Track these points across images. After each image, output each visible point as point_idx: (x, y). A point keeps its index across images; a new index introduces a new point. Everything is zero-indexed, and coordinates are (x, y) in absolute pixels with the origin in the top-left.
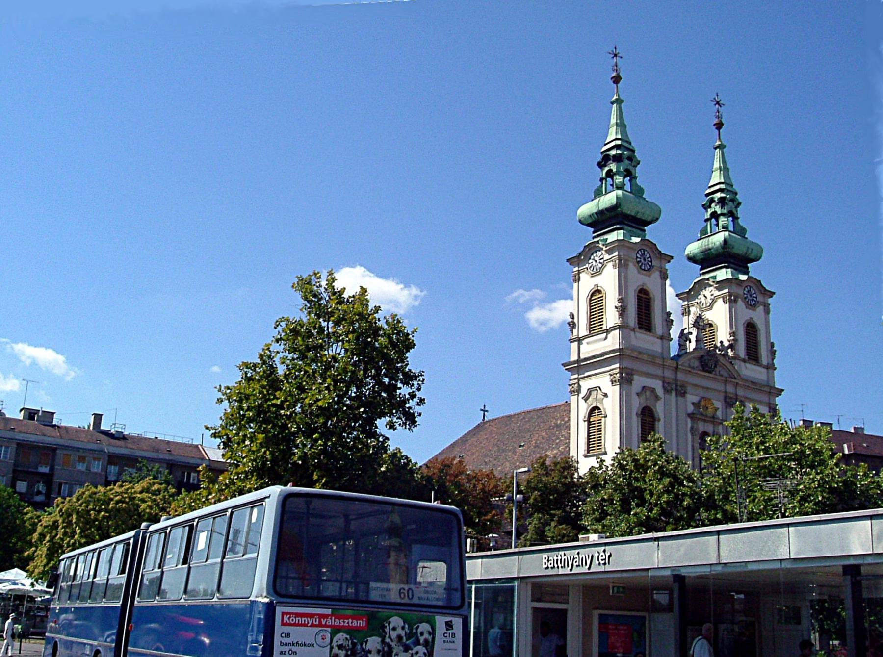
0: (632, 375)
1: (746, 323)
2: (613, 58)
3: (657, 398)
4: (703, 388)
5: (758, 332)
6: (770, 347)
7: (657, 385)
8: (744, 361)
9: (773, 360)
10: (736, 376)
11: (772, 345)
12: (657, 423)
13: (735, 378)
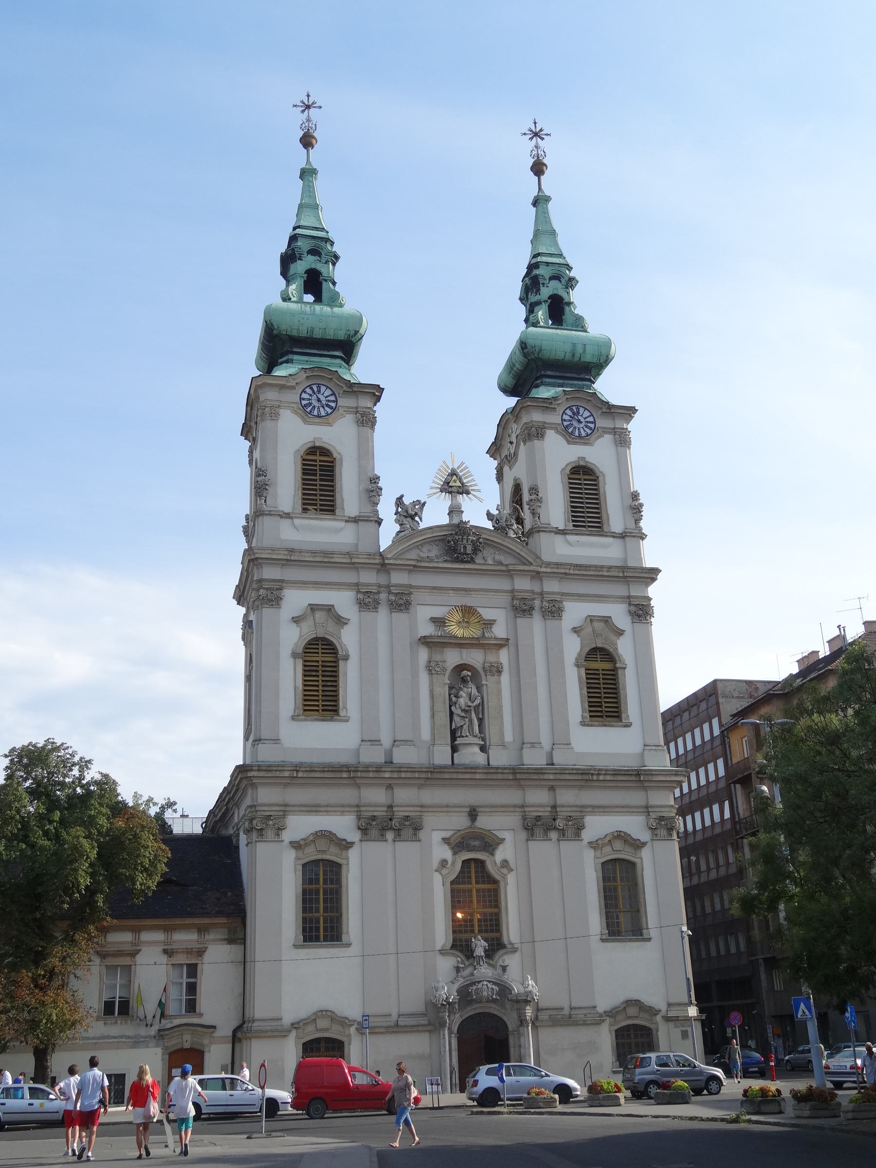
0: (281, 589)
1: (569, 468)
2: (303, 111)
3: (341, 621)
5: (601, 479)
6: (629, 501)
8: (563, 532)
9: (638, 520)
10: (530, 560)
11: (635, 496)
12: (341, 663)
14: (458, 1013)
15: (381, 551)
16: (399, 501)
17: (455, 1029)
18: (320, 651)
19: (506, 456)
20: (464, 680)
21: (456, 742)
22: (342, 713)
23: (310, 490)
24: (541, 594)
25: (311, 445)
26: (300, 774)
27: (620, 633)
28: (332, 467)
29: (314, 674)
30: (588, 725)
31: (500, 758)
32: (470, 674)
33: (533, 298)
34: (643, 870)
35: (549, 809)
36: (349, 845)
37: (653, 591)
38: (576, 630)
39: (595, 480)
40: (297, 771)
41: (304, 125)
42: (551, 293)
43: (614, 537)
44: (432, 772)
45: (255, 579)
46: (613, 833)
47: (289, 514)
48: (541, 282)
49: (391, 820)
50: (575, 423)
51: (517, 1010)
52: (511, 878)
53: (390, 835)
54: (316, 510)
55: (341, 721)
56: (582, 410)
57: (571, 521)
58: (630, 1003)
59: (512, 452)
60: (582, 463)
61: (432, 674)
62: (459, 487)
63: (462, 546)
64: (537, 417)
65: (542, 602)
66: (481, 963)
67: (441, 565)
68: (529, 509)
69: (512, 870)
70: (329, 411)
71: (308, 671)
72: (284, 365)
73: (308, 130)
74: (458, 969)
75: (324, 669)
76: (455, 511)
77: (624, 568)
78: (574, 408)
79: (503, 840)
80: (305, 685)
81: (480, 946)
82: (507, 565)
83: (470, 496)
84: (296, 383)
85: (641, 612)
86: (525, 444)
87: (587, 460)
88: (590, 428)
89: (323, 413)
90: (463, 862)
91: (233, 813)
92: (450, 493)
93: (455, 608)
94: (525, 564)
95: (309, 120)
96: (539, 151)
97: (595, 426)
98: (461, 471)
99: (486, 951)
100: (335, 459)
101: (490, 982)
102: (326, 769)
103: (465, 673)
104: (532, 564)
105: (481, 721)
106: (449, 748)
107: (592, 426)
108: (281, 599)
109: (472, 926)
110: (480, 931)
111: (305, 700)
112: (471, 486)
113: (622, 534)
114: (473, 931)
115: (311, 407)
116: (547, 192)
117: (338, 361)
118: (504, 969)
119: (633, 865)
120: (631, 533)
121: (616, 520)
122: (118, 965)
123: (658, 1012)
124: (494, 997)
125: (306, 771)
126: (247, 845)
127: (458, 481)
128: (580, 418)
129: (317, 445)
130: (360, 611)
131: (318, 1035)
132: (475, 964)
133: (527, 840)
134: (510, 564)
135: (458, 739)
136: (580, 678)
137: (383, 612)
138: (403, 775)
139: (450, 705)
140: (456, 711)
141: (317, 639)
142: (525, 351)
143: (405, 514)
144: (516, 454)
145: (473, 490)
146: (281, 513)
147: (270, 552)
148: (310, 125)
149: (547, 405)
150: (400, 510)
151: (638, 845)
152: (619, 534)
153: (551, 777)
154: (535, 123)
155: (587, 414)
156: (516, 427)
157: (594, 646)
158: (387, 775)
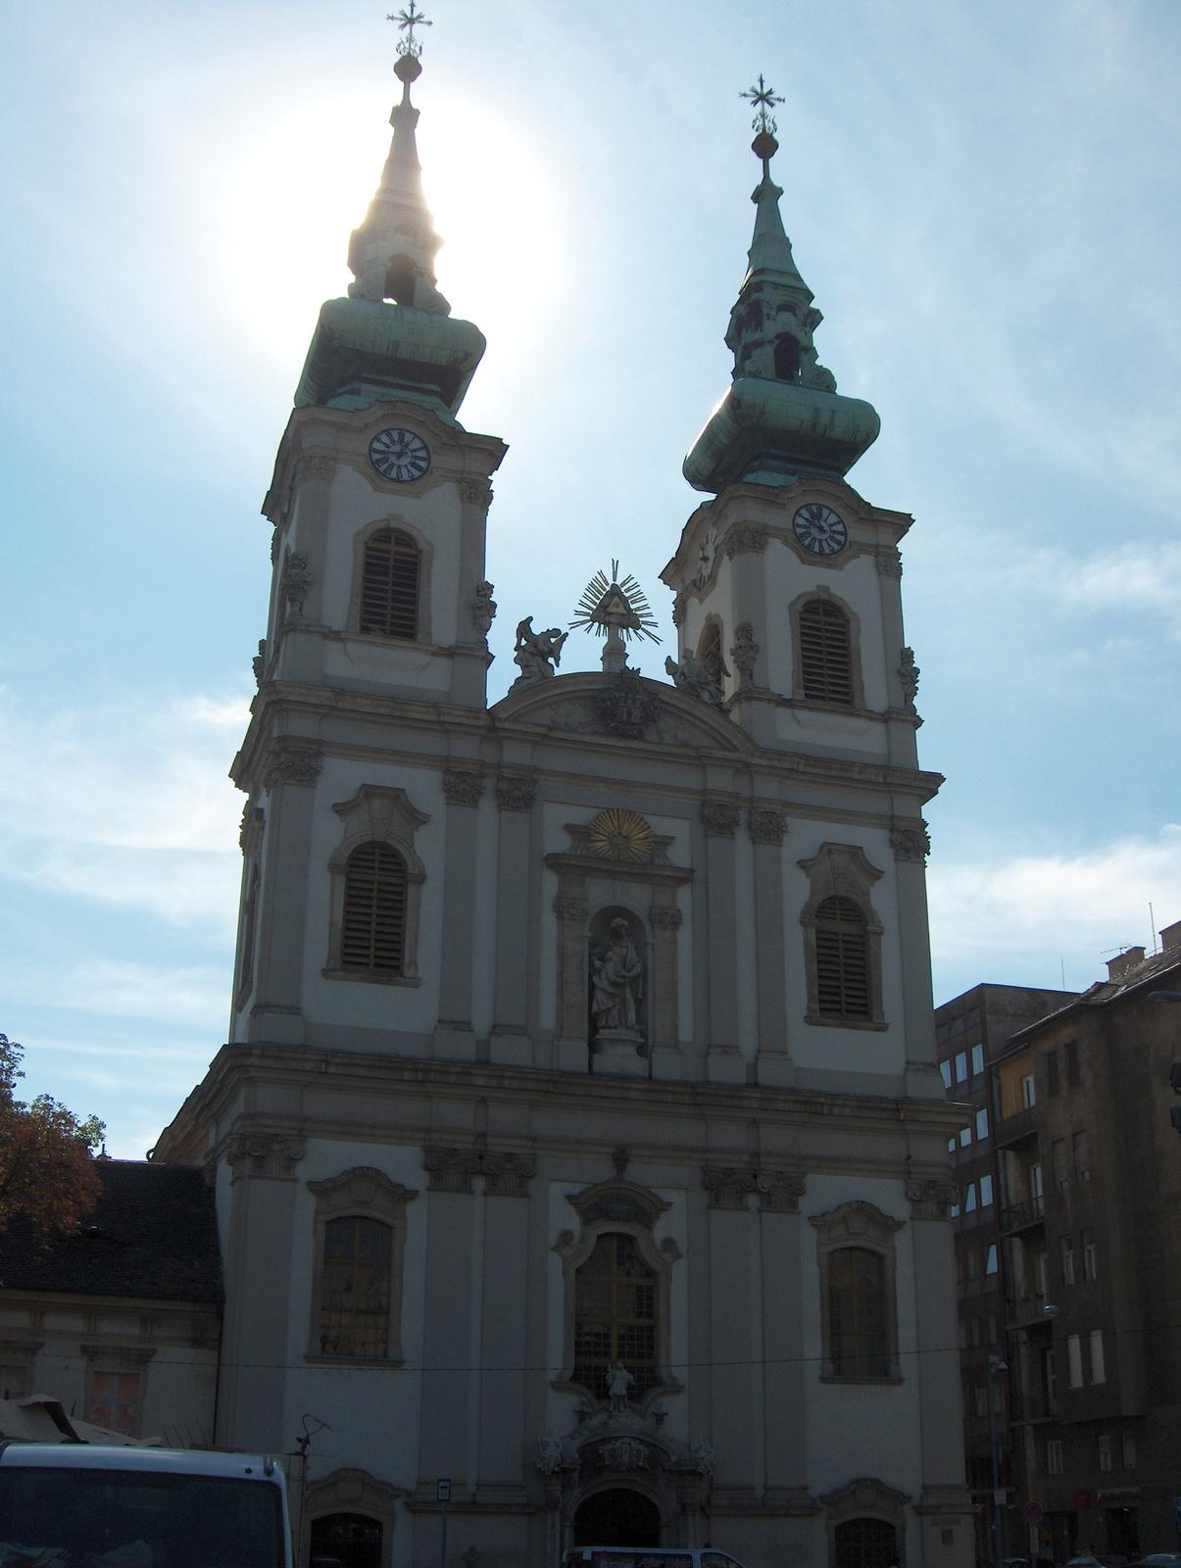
0: (319, 754)
3: (416, 818)
4: (610, 782)
5: (853, 624)
7: (423, 786)
8: (790, 704)
11: (907, 655)
12: (411, 889)
13: (737, 750)
15: (488, 708)
16: (524, 628)
17: (572, 1513)
18: (377, 865)
19: (694, 581)
20: (616, 934)
21: (598, 1037)
22: (408, 972)
23: (376, 590)
24: (751, 800)
25: (382, 525)
26: (332, 1069)
27: (877, 875)
28: (416, 564)
29: (364, 902)
30: (817, 1024)
31: (666, 1066)
32: (626, 923)
33: (749, 337)
34: (895, 1268)
35: (746, 1158)
36: (410, 1195)
37: (928, 811)
38: (803, 865)
39: (843, 626)
40: (328, 1063)
41: (402, 46)
42: (780, 331)
43: (871, 719)
44: (555, 1082)
45: (275, 735)
46: (849, 1204)
47: (339, 633)
48: (765, 311)
49: (481, 1158)
50: (814, 532)
52: (679, 1270)
53: (479, 1183)
54: (384, 631)
55: (405, 985)
56: (825, 513)
57: (802, 686)
58: (862, 1483)
59: (706, 572)
60: (824, 596)
61: (563, 918)
62: (623, 615)
63: (625, 710)
64: (754, 514)
65: (751, 814)
66: (622, 1408)
67: (587, 739)
68: (735, 662)
69: (679, 1256)
70: (417, 473)
71: (355, 898)
72: (346, 396)
73: (409, 53)
74: (582, 1416)
75: (382, 895)
76: (615, 652)
77: (887, 769)
78: (814, 508)
79: (666, 1206)
80: (347, 921)
81: (620, 1381)
82: (697, 748)
83: (640, 632)
84: (366, 424)
85: (910, 844)
86: (731, 558)
87: (833, 590)
88: (838, 542)
89: (405, 476)
90: (599, 1237)
91: (208, 1133)
92: (607, 624)
93: (608, 813)
94: (725, 748)
95: (410, 40)
96: (766, 121)
97: (846, 539)
98: (627, 591)
99: (630, 1388)
100: (421, 551)
102: (377, 1064)
103: (618, 921)
104: (738, 750)
105: (640, 1003)
106: (586, 1044)
107: (841, 538)
108: (318, 772)
109: (609, 1346)
110: (621, 1355)
111: (346, 946)
112: (642, 616)
113: (883, 714)
114: (607, 1354)
115: (387, 465)
116: (777, 180)
117: (437, 400)
118: (660, 1418)
119: (880, 1258)
120: (898, 714)
121: (875, 690)
122: (3, 1366)
123: (908, 1498)
124: (641, 1464)
125: (342, 1064)
126: (232, 1184)
127: (621, 606)
128: (823, 524)
129: (393, 525)
130: (447, 804)
131: (337, 1510)
132: (611, 1409)
133: (709, 1207)
134: (702, 747)
135: (601, 1031)
136: (807, 943)
137: (487, 807)
138: (507, 1083)
139: (589, 974)
140: (601, 982)
141: (372, 844)
142: (738, 412)
143: (532, 649)
144: (713, 577)
145: (646, 623)
146: (326, 631)
147: (303, 691)
148: (412, 47)
149: (773, 498)
150: (524, 642)
151: (891, 1226)
152: (880, 714)
153: (755, 1104)
154: (762, 82)
155: (833, 519)
156: (715, 533)
157: (832, 893)
158: (481, 1081)
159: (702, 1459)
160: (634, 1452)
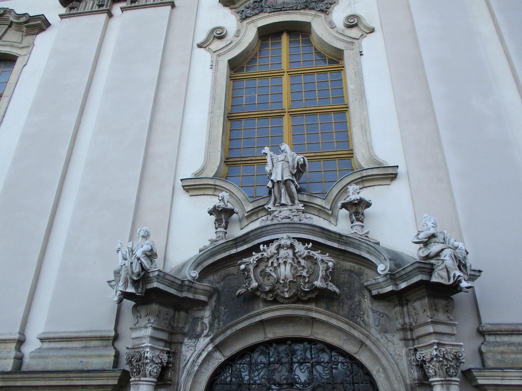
14: (207, 336)
51: (404, 329)
69: (372, 31)
101: (304, 241)
124: (318, 283)
159: (438, 254)
160: (303, 262)
